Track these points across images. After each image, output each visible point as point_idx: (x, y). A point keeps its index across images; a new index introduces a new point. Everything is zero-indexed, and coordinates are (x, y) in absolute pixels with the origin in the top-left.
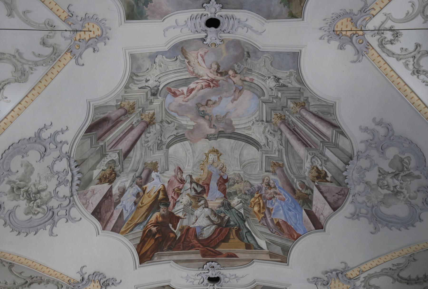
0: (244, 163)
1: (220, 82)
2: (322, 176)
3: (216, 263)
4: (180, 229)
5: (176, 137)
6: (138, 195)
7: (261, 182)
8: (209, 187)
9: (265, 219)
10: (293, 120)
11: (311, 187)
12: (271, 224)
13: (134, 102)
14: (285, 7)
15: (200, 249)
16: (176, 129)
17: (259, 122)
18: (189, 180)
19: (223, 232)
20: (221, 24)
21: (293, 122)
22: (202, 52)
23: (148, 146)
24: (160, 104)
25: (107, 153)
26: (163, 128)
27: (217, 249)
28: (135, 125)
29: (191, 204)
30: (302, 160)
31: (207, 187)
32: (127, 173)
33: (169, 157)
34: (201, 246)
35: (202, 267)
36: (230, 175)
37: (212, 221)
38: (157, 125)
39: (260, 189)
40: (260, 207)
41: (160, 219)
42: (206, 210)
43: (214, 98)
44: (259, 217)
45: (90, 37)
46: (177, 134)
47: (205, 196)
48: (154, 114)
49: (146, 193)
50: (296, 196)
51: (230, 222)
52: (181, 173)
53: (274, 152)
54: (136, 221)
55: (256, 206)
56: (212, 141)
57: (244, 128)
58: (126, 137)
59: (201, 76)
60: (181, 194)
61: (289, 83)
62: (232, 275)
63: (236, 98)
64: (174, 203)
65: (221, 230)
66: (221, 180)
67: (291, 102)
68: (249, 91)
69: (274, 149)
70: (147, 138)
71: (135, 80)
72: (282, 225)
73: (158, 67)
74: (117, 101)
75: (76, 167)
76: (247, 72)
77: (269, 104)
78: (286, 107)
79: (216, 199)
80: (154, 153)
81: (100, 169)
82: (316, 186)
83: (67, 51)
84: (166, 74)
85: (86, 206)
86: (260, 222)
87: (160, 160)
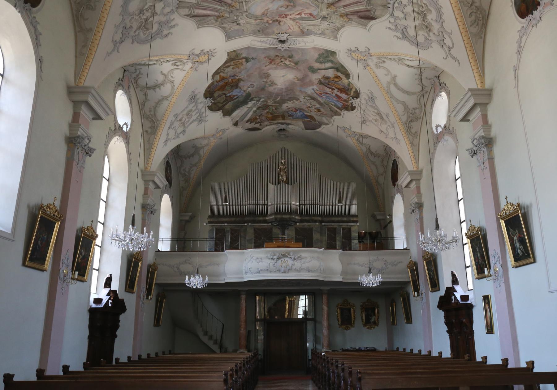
21: (223, 7)
38: (326, 2)
48: (327, 8)
58: (350, 3)
61: (230, 25)
73: (321, 29)
78: (230, 13)
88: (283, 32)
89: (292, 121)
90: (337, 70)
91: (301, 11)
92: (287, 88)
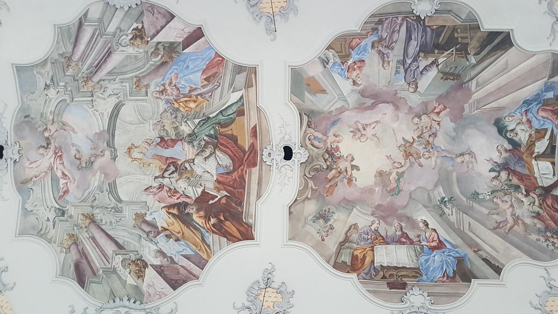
3: (265, 150)
4: (217, 191)
5: (111, 192)
8: (170, 158)
9: (203, 94)
10: (86, 69)
11: (154, 44)
12: (209, 88)
13: (67, 234)
15: (245, 169)
16: (102, 192)
17: (94, 104)
18: (160, 180)
19: (224, 142)
23: (116, 222)
25: (112, 267)
27: (247, 149)
28: (91, 235)
29: (189, 178)
30: (127, 56)
32: (141, 247)
33: (132, 200)
34: (242, 167)
35: (269, 166)
36: (156, 135)
37: (211, 154)
39: (168, 102)
40: (190, 101)
41: (202, 213)
42: (196, 161)
43: (73, 152)
44: (202, 101)
47: (180, 163)
49: (167, 227)
50: (169, 60)
51: (212, 135)
52: (151, 188)
53: (123, 88)
54: (199, 241)
55: (188, 106)
57: (101, 120)
59: (50, 165)
60: (175, 189)
61: (48, 75)
62: (281, 131)
65: (222, 145)
67: (67, 71)
68: (63, 116)
69: (120, 87)
70: (107, 223)
71: (45, 232)
72: (208, 75)
73: (37, 208)
76: (44, 117)
77: (73, 94)
78: (74, 76)
82: (151, 39)
84: (44, 200)
85: (163, 296)
86: (208, 101)
87: (134, 210)
88: (21, 152)
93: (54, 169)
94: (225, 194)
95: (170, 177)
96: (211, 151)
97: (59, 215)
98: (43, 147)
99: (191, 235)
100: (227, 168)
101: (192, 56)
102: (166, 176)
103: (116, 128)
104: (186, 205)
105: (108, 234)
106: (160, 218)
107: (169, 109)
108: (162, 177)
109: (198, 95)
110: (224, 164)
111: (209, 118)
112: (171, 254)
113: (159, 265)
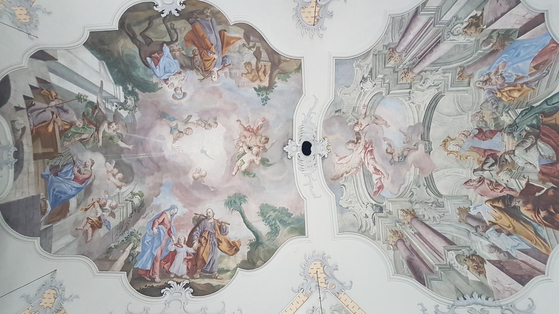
0: (459, 110)
1: (367, 140)
2: (475, 21)
4: (542, 183)
5: (428, 186)
6: (499, 231)
7: (482, 90)
8: (488, 150)
9: (529, 83)
10: (409, 59)
11: (489, 32)
12: (537, 76)
13: (390, 231)
14: (290, 77)
16: (419, 187)
17: (411, 96)
18: (480, 173)
20: (308, 140)
22: (337, 159)
23: (439, 217)
24: (392, 204)
25: (448, 263)
26: (419, 201)
28: (416, 231)
29: (510, 171)
30: (456, 45)
31: (487, 152)
32: (472, 242)
33: (452, 194)
36: (474, 126)
37: (532, 145)
38: (414, 207)
39: (490, 91)
40: (514, 90)
41: (530, 206)
42: (517, 152)
43: (385, 146)
45: (322, 273)
46: (424, 186)
47: (499, 155)
49: (495, 222)
50: (500, 48)
51: (534, 125)
52: (471, 182)
53: (446, 78)
55: (512, 95)
56: (433, 147)
57: (417, 112)
59: (361, 160)
60: (496, 182)
61: (367, 67)
63: (384, 123)
64: (509, 189)
65: (544, 134)
66: (480, 137)
71: (366, 229)
72: (538, 63)
74: (389, 249)
75: (465, 299)
76: (356, 111)
78: (394, 68)
79: (503, 141)
80: (448, 212)
81: (467, 272)
82: (487, 27)
83: (338, 298)
84: (359, 196)
85: (513, 292)
86: (533, 89)
87: (456, 205)
89: (32, 175)
90: (256, 244)
91: (384, 173)
92: (163, 159)
93: (365, 165)
94: (552, 186)
95: (489, 169)
96: (533, 142)
97: (377, 211)
98: (353, 142)
99: (523, 229)
100: (550, 159)
101: (526, 44)
102: (485, 169)
103: (432, 120)
104: (511, 198)
105: (434, 229)
106: (486, 212)
107: (490, 99)
108: (481, 169)
109: (524, 83)
110: (547, 154)
111: (532, 107)
112: (507, 249)
113: (497, 260)
